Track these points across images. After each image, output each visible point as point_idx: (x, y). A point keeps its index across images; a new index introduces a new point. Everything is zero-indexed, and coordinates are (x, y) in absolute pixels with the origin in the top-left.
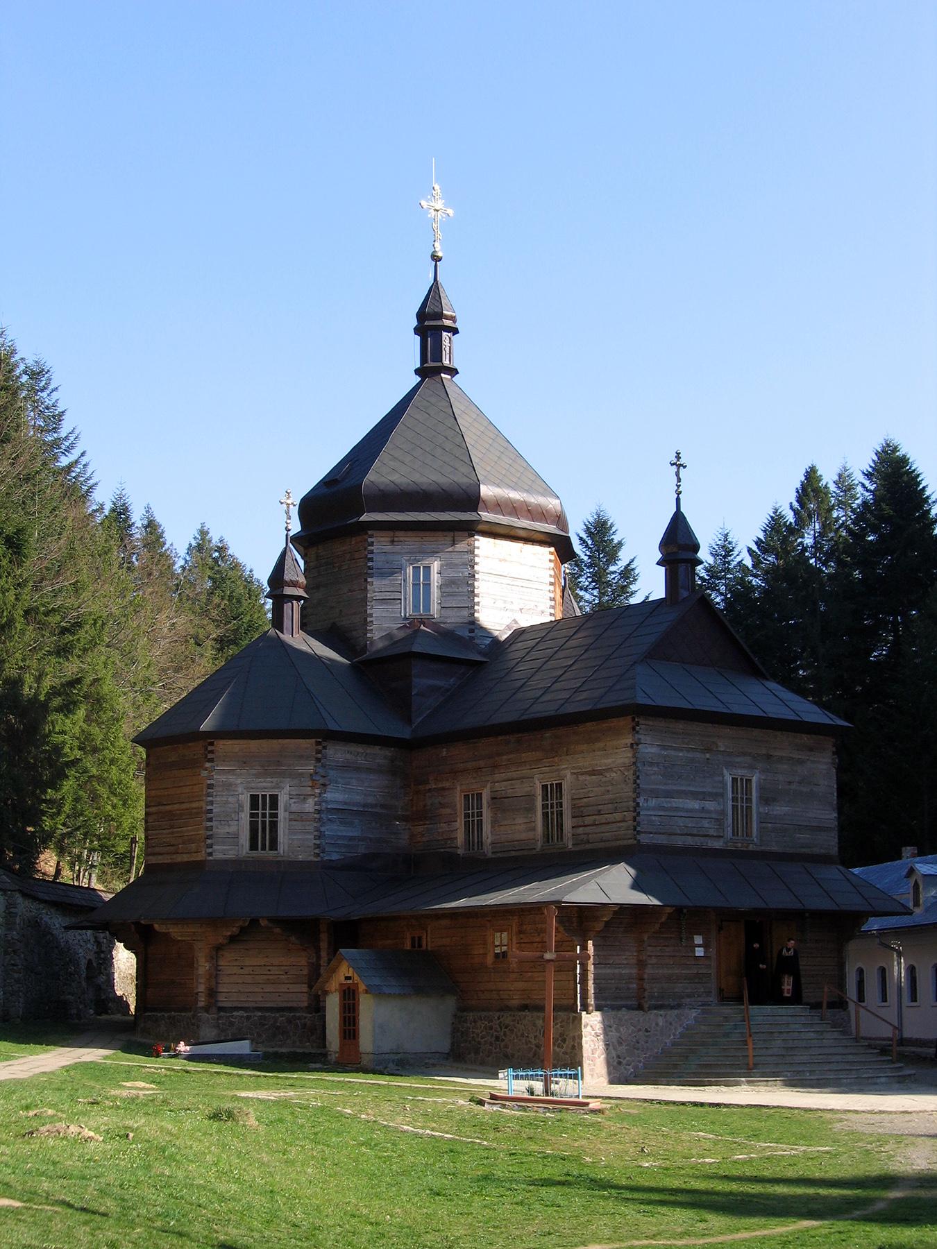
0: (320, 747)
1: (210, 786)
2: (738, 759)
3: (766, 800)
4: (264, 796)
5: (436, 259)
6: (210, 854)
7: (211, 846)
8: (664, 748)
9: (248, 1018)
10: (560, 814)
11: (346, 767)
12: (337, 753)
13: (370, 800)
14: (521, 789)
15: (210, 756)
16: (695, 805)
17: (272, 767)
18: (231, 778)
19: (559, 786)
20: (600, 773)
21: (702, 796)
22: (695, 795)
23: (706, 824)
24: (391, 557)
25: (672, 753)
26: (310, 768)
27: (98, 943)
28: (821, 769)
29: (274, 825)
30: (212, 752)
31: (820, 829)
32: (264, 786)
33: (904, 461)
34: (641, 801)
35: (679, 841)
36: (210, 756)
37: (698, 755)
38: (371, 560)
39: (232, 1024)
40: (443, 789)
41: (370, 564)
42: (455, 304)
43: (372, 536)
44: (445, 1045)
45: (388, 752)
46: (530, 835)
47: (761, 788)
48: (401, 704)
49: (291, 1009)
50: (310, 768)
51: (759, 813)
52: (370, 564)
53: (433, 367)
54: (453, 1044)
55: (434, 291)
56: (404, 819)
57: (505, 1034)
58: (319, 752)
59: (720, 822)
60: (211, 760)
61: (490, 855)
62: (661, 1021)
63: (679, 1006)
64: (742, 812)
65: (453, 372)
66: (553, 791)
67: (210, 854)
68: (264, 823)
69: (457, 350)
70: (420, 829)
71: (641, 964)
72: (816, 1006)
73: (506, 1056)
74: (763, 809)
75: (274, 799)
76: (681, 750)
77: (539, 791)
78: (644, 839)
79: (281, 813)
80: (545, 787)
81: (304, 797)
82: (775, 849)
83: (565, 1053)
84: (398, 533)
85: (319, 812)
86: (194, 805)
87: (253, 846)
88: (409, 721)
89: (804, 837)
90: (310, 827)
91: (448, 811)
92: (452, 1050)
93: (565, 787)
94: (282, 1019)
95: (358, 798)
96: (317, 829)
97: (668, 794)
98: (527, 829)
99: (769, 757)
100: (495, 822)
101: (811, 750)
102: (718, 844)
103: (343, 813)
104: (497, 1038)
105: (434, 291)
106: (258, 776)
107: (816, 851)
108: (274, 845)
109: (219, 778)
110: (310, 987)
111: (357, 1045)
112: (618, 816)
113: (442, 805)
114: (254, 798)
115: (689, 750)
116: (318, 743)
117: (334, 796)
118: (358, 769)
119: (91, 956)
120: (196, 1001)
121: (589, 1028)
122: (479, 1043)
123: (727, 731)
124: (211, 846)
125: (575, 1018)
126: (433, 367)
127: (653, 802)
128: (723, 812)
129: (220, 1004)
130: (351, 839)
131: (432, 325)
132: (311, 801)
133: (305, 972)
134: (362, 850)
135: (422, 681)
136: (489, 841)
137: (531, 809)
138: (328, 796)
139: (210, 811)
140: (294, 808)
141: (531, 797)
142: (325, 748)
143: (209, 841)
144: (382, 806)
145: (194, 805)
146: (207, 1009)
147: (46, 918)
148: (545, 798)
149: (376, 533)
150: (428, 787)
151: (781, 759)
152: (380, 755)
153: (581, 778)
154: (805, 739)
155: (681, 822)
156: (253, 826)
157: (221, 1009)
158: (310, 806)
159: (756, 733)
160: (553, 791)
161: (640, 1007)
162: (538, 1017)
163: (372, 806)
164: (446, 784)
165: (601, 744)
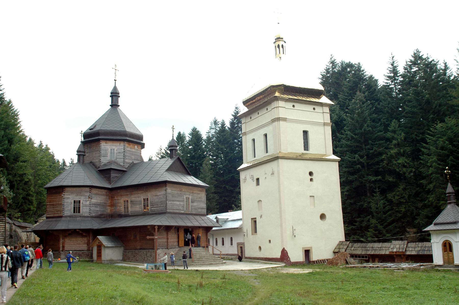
1: (64, 198)
3: (192, 202)
5: (115, 80)
8: (172, 190)
11: (96, 194)
12: (94, 191)
13: (102, 202)
14: (138, 199)
16: (178, 203)
17: (78, 194)
19: (148, 199)
22: (178, 201)
23: (180, 207)
27: (27, 235)
28: (203, 195)
29: (79, 207)
31: (203, 208)
32: (77, 199)
33: (198, 131)
35: (175, 211)
42: (120, 90)
45: (106, 191)
47: (191, 199)
48: (109, 180)
49: (83, 250)
53: (115, 105)
55: (115, 88)
56: (109, 206)
64: (188, 204)
65: (119, 106)
66: (146, 200)
69: (121, 101)
72: (204, 247)
73: (136, 260)
74: (192, 204)
75: (79, 201)
77: (143, 200)
78: (168, 211)
81: (86, 201)
87: (74, 212)
88: (111, 184)
89: (200, 210)
90: (88, 208)
93: (149, 199)
94: (81, 253)
95: (99, 201)
97: (173, 201)
98: (138, 208)
100: (131, 207)
102: (183, 212)
103: (96, 205)
105: (115, 88)
107: (202, 213)
108: (79, 212)
109: (66, 196)
111: (101, 258)
112: (162, 206)
113: (118, 203)
114: (75, 201)
117: (94, 201)
118: (99, 195)
120: (60, 249)
123: (184, 187)
126: (115, 105)
127: (170, 202)
128: (184, 205)
131: (115, 95)
134: (99, 213)
135: (113, 175)
138: (92, 201)
140: (84, 203)
141: (141, 201)
146: (62, 251)
151: (195, 193)
152: (104, 192)
154: (200, 189)
156: (74, 207)
157: (66, 251)
158: (88, 203)
159: (190, 187)
160: (146, 200)
161: (167, 248)
164: (119, 198)
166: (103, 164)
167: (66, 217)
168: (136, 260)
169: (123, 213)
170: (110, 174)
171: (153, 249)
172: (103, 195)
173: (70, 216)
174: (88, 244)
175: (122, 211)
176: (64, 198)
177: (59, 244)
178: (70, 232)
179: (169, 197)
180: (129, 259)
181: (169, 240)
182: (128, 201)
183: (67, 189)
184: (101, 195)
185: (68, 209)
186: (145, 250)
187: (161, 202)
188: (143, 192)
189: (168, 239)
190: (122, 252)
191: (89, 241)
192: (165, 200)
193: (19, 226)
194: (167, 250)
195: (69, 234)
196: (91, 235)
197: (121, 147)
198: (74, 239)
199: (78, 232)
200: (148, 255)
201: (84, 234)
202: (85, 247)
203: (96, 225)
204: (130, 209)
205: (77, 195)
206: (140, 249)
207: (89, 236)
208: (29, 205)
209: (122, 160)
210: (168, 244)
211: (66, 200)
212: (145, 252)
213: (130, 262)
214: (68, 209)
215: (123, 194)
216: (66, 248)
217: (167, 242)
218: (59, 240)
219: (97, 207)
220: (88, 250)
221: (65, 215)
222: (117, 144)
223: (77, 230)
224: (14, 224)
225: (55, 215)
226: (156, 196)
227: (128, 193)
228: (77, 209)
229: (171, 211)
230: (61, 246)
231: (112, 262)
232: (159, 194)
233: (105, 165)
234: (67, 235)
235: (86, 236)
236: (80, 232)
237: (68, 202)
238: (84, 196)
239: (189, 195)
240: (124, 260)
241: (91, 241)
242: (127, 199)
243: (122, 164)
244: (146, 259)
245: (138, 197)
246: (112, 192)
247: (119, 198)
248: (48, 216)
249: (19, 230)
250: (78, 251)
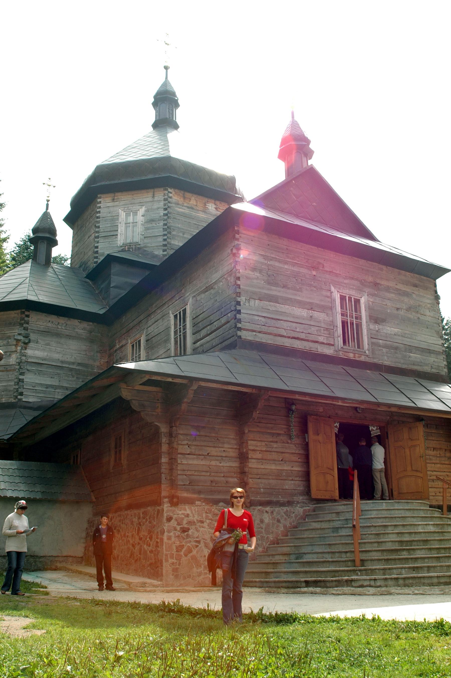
2: (346, 281)
3: (375, 319)
5: (166, 68)
16: (304, 313)
21: (311, 307)
22: (301, 304)
23: (313, 330)
24: (111, 209)
25: (277, 264)
31: (430, 352)
37: (303, 271)
38: (99, 212)
41: (98, 215)
43: (100, 198)
47: (369, 308)
51: (369, 330)
52: (98, 215)
59: (330, 330)
62: (267, 518)
71: (243, 457)
76: (286, 263)
78: (245, 335)
82: (387, 363)
83: (151, 552)
84: (117, 194)
89: (415, 356)
99: (376, 285)
101: (415, 286)
102: (329, 351)
107: (427, 369)
112: (223, 320)
115: (294, 264)
121: (173, 523)
123: (331, 255)
138: (29, 352)
142: (28, 316)
144: (79, 364)
149: (102, 196)
150: (115, 349)
151: (388, 289)
163: (69, 363)
172: (77, 338)
181: (252, 464)
189: (243, 457)
197: (156, 206)
209: (161, 239)
212: (135, 520)
222: (146, 196)
239: (360, 290)
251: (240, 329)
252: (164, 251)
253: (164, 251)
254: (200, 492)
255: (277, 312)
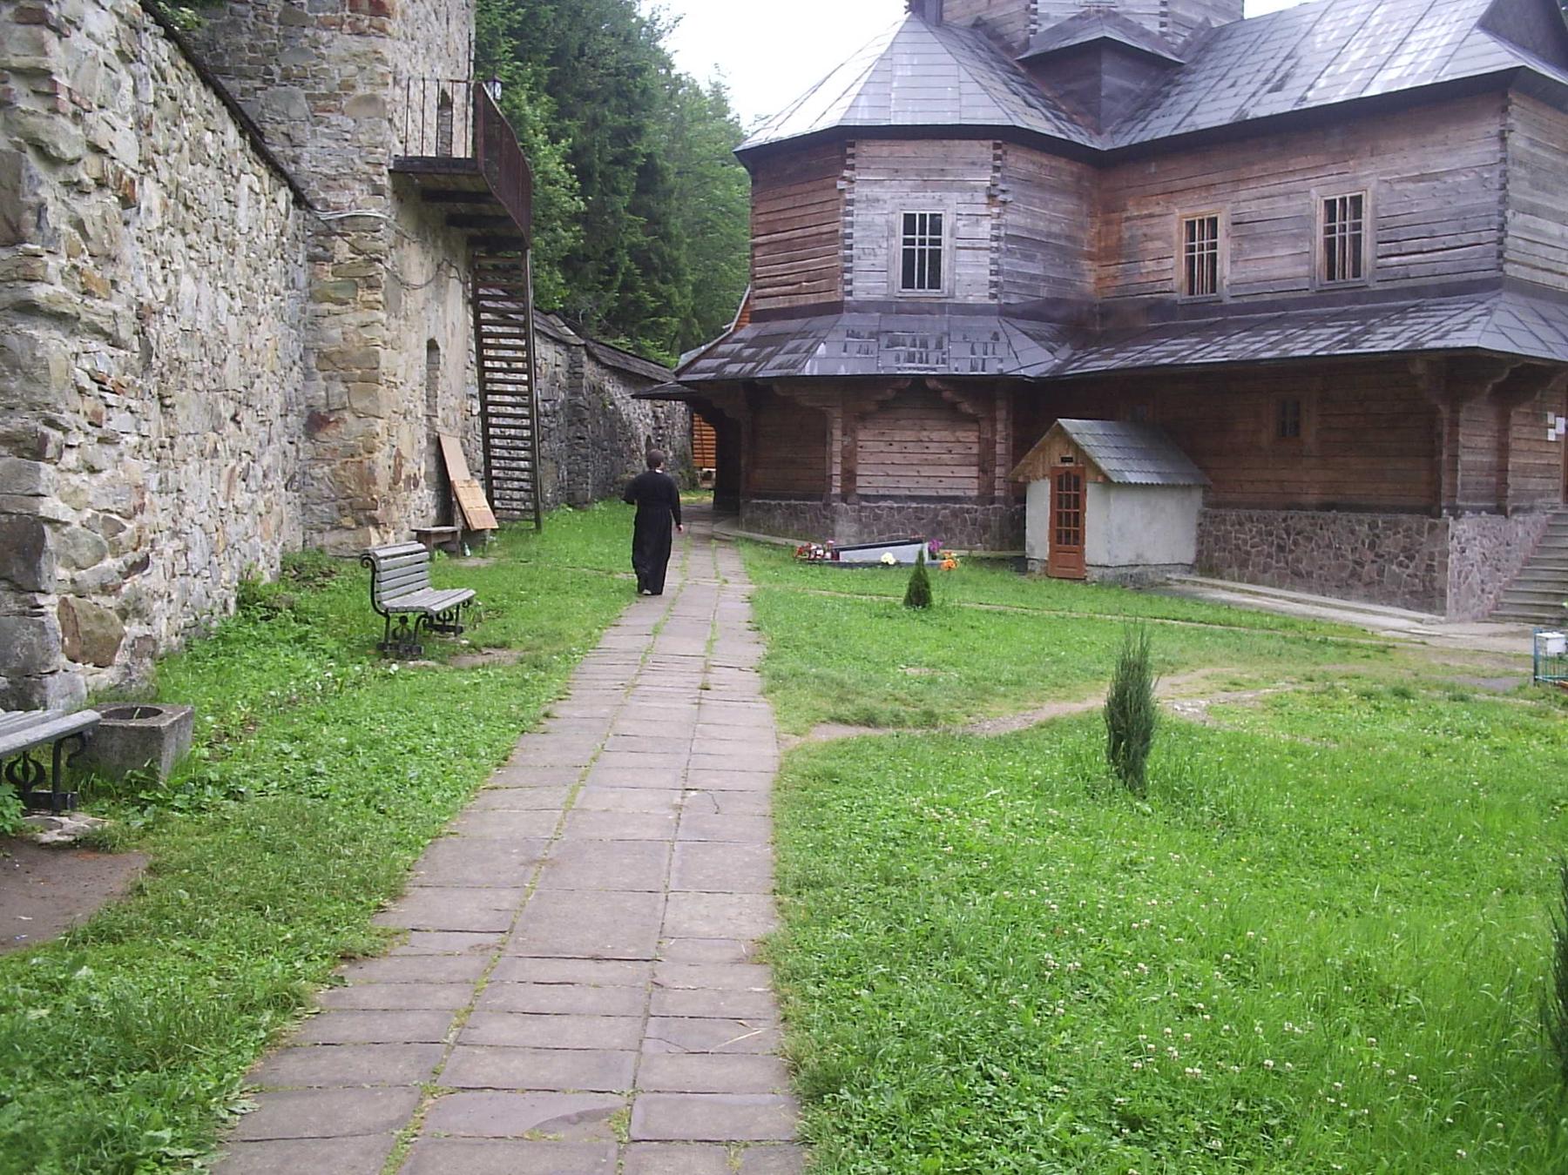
0: (999, 152)
1: (851, 202)
4: (923, 217)
6: (850, 293)
7: (850, 282)
9: (900, 510)
10: (1357, 240)
11: (1027, 182)
13: (1055, 228)
14: (1283, 207)
15: (849, 162)
18: (877, 191)
19: (1357, 201)
20: (1435, 177)
26: (985, 178)
27: (656, 417)
29: (936, 256)
30: (852, 156)
32: (923, 204)
34: (1509, 213)
36: (849, 162)
39: (878, 518)
40: (1151, 216)
44: (1189, 556)
45: (1075, 168)
46: (1302, 270)
48: (1087, 107)
49: (956, 499)
50: (985, 178)
54: (1199, 553)
56: (1090, 257)
57: (1295, 543)
58: (997, 157)
60: (852, 168)
61: (1228, 301)
63: (1531, 509)
67: (850, 293)
68: (922, 252)
70: (1112, 269)
73: (1298, 574)
75: (936, 223)
77: (1321, 212)
79: (945, 237)
80: (1330, 205)
85: (997, 238)
86: (825, 229)
87: (907, 282)
90: (985, 258)
91: (1159, 244)
92: (1197, 560)
93: (1367, 204)
94: (944, 512)
95: (1041, 225)
96: (994, 262)
97: (1533, 211)
98: (1288, 263)
103: (1022, 243)
104: (1281, 548)
106: (915, 189)
108: (935, 283)
109: (861, 192)
110: (983, 471)
111: (1081, 553)
112: (1468, 239)
114: (909, 219)
116: (997, 146)
117: (1016, 219)
118: (1041, 186)
119: (650, 432)
122: (1248, 553)
124: (850, 282)
125: (1432, 527)
127: (1521, 218)
129: (860, 491)
130: (1033, 277)
132: (987, 224)
133: (975, 450)
135: (1113, 79)
136: (1226, 282)
137: (1304, 235)
138: (1008, 218)
139: (850, 236)
140: (963, 232)
141: (1305, 220)
142: (1005, 153)
143: (847, 276)
144: (1068, 238)
145: (825, 229)
147: (608, 387)
148: (1331, 216)
153: (1398, 187)
155: (1543, 251)
156: (908, 256)
157: (866, 498)
158: (985, 229)
161: (1500, 510)
162: (1360, 523)
163: (1057, 236)
164: (1157, 210)
165: (1440, 137)
166: (1048, 25)
167: (862, 308)
168: (1298, 574)
169: (1182, 296)
170: (1096, 73)
171: (1432, 510)
173: (885, 307)
174: (985, 465)
175: (1175, 284)
176: (851, 202)
177: (825, 458)
178: (890, 393)
179: (1520, 191)
180: (1243, 565)
181: (1514, 461)
182: (1213, 222)
183: (867, 149)
184: (1054, 189)
185: (874, 270)
186: (1366, 517)
187: (1461, 215)
188: (1320, 159)
189: (1503, 450)
190: (1194, 519)
191: (988, 446)
192: (1492, 199)
193: (616, 371)
194: (1501, 518)
195: (884, 407)
196: (1001, 414)
198: (910, 435)
199: (937, 392)
200: (1389, 545)
201: (967, 407)
202: (963, 481)
203: (1032, 359)
204: (1225, 270)
205: (925, 185)
206: (1327, 507)
207: (993, 421)
208: (664, 281)
210: (1503, 483)
211: (861, 215)
213: (1252, 581)
214: (874, 270)
215: (1180, 184)
216: (863, 485)
217: (1502, 470)
218: (823, 438)
219: (1030, 258)
220: (986, 497)
221: (860, 296)
223: (930, 384)
224: (591, 356)
225: (801, 301)
226: (1421, 178)
227: (1215, 178)
228: (922, 264)
229: (1524, 273)
230: (837, 470)
231: (1136, 581)
232: (1440, 163)
233: (1058, 30)
234: (871, 407)
235: (974, 419)
236: (947, 395)
237: (869, 226)
238: (963, 188)
240: (1206, 565)
241: (999, 449)
242: (1205, 211)
243: (1153, 27)
244: (1369, 570)
245: (1288, 195)
246: (1107, 175)
247: (1157, 210)
248: (761, 305)
249: (618, 393)
250: (929, 499)
251: (1506, 261)
252: (1163, 25)
253: (1163, 25)
254: (1467, 498)
255: (1539, 232)
